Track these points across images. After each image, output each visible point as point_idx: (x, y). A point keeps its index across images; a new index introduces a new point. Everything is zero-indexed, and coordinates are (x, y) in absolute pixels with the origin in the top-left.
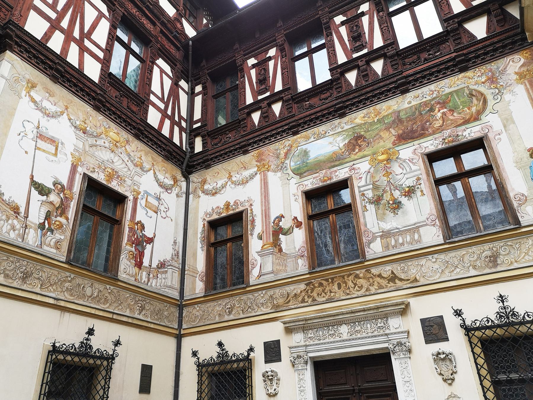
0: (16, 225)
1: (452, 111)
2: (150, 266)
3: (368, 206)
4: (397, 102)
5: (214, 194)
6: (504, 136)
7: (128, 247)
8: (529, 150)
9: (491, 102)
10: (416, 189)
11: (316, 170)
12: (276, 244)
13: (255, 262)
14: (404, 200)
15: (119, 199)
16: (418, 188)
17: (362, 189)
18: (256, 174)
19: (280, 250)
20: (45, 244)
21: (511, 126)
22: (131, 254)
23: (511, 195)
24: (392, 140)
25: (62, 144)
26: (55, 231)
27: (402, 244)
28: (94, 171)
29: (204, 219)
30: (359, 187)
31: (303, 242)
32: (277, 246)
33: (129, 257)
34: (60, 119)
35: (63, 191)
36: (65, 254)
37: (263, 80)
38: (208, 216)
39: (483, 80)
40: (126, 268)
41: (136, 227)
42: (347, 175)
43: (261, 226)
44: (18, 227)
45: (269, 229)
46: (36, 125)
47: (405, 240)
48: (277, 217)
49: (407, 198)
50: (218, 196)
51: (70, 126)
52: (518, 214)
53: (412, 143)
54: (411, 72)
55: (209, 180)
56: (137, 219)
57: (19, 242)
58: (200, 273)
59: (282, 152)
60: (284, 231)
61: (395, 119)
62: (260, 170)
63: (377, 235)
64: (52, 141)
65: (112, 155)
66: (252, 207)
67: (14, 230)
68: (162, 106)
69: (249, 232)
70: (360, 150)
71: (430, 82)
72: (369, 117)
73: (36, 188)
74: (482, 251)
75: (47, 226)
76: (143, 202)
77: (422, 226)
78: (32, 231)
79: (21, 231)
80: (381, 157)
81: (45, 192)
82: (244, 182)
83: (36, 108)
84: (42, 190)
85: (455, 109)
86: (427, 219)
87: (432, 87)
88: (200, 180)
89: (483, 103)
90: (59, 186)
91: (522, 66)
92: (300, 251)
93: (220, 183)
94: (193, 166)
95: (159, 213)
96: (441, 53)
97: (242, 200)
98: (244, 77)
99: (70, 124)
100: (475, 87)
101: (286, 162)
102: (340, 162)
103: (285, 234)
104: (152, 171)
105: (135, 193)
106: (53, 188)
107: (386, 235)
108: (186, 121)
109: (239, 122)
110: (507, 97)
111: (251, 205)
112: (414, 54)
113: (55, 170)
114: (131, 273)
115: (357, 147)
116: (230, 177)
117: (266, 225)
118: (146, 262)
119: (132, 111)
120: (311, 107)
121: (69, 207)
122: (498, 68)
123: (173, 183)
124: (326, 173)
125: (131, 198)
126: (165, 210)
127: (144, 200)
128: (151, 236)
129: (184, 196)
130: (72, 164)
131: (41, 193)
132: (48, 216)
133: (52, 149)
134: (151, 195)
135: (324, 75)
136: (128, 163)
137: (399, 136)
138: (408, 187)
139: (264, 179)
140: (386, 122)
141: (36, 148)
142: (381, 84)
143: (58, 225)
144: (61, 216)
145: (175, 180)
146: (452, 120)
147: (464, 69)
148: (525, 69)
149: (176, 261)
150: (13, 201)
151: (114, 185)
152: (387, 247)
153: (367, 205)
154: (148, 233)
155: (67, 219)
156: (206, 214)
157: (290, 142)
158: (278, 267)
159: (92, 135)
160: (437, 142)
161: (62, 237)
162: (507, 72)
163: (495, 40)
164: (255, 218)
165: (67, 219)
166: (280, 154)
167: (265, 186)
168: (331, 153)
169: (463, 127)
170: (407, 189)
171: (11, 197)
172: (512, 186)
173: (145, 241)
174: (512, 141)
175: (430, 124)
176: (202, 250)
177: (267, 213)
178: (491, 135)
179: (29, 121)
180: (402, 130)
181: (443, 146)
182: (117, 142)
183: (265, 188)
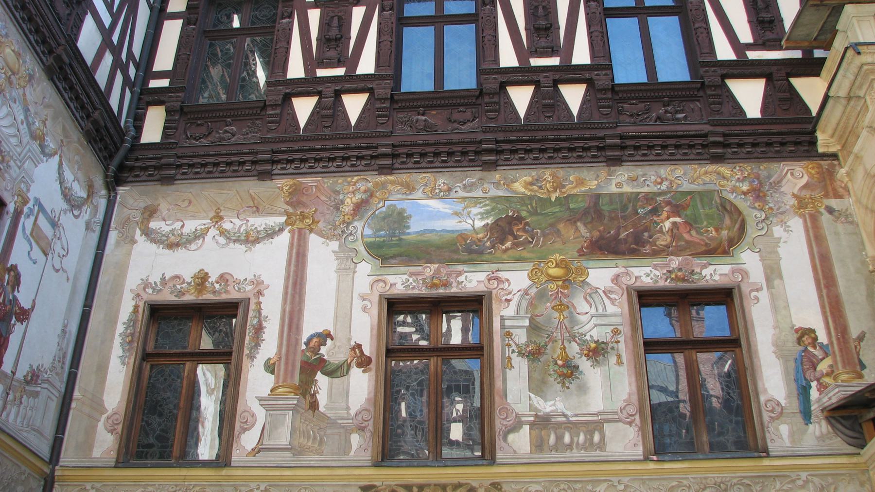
1: (690, 224)
2: (14, 373)
3: (516, 360)
4: (598, 176)
5: (172, 246)
6: (764, 295)
8: (797, 331)
9: (751, 232)
10: (609, 350)
11: (419, 259)
12: (305, 389)
13: (250, 419)
14: (585, 364)
16: (613, 348)
17: (508, 323)
18: (281, 230)
19: (314, 406)
21: (776, 282)
23: (763, 399)
24: (580, 247)
27: (570, 447)
29: (138, 295)
30: (502, 318)
31: (368, 400)
32: (308, 397)
37: (334, 43)
38: (150, 291)
39: (745, 188)
41: (7, 277)
42: (482, 288)
43: (275, 343)
45: (295, 354)
47: (575, 439)
48: (318, 335)
49: (589, 363)
50: (180, 252)
52: (767, 435)
53: (615, 262)
54: (632, 130)
55: (165, 213)
56: (12, 261)
58: (110, 412)
59: (348, 200)
60: (330, 368)
61: (589, 207)
62: (293, 224)
63: (523, 419)
66: (261, 299)
68: (107, 20)
69: (246, 351)
70: (516, 245)
71: (659, 160)
72: (540, 187)
74: (702, 486)
77: (609, 421)
80: (554, 272)
82: (250, 239)
85: (696, 222)
86: (621, 410)
87: (664, 170)
88: (142, 205)
89: (739, 229)
91: (806, 186)
92: (359, 418)
93: (191, 226)
94: (132, 169)
95: (50, 256)
96: (685, 117)
97: (239, 275)
98: (291, 16)
100: (731, 197)
101: (356, 224)
102: (470, 257)
103: (330, 373)
104: (57, 157)
107: (542, 422)
108: (137, 67)
109: (264, 107)
110: (778, 231)
111: (260, 293)
112: (641, 100)
115: (510, 237)
116: (218, 218)
117: (288, 346)
119: (57, 14)
120: (428, 127)
122: (769, 177)
123: (85, 196)
124: (438, 271)
125: (11, 207)
126: (63, 253)
127: (32, 218)
128: (26, 304)
129: (98, 229)
135: (461, 76)
136: (21, 127)
137: (591, 241)
138: (596, 342)
139: (299, 245)
140: (572, 206)
142: (575, 134)
145: (91, 191)
146: (687, 242)
147: (717, 159)
148: (807, 194)
149: (57, 374)
152: (538, 445)
153: (514, 356)
156: (146, 285)
157: (370, 185)
158: (303, 441)
160: (658, 273)
162: (783, 189)
163: (775, 129)
164: (265, 324)
166: (342, 202)
167: (297, 261)
168: (455, 235)
169: (704, 261)
170: (593, 345)
172: (764, 385)
173: (16, 314)
174: (775, 309)
175: (651, 237)
176: (123, 363)
177: (295, 320)
178: (745, 289)
180: (599, 231)
181: (667, 284)
182: (13, 73)
183: (297, 266)
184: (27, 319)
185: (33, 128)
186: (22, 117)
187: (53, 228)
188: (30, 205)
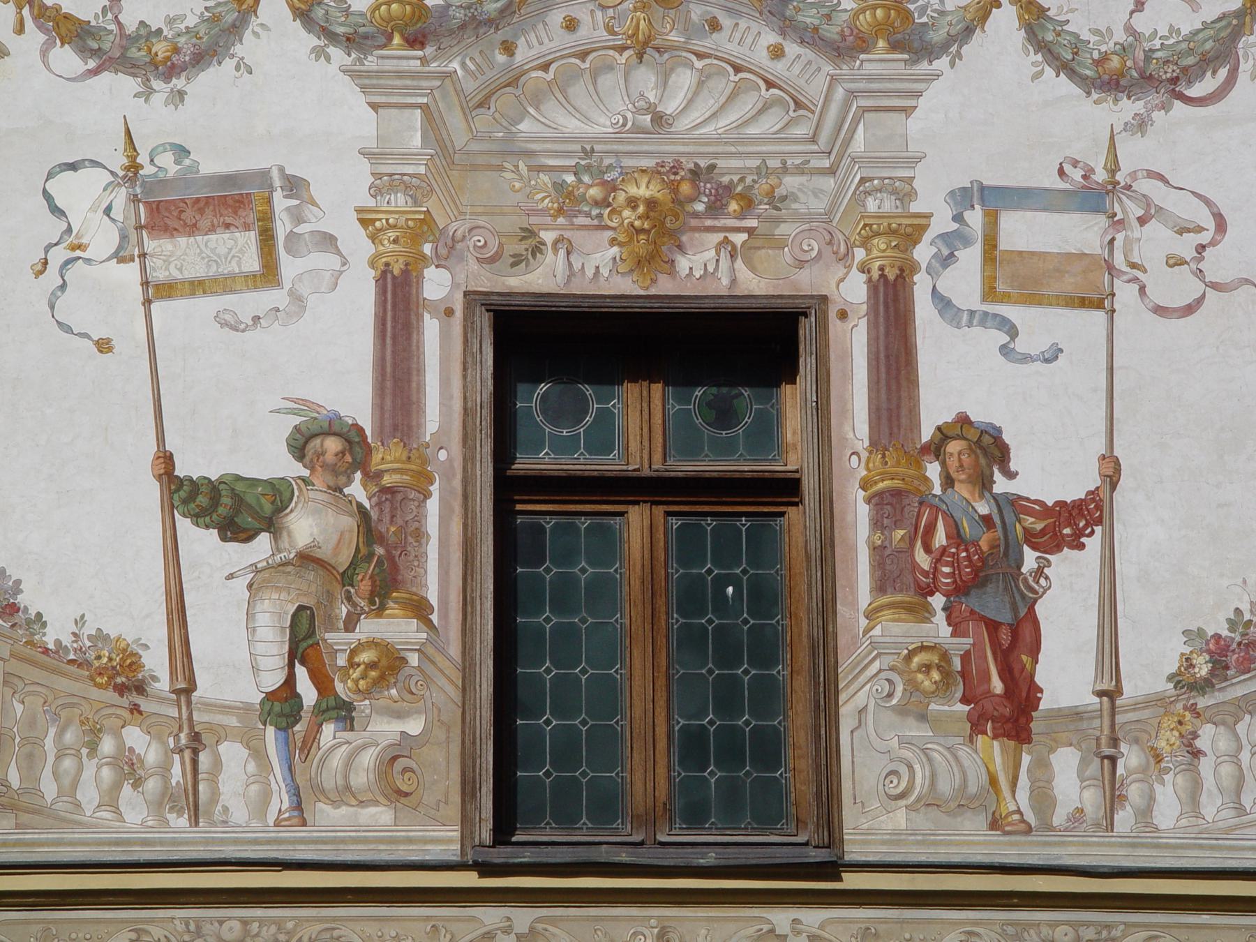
0: (140, 750)
2: (1111, 695)
7: (896, 631)
15: (756, 346)
20: (320, 792)
22: (927, 668)
25: (294, 185)
26: (363, 705)
28: (537, 249)
33: (913, 687)
34: (247, 47)
35: (362, 463)
36: (453, 809)
40: (896, 771)
41: (933, 470)
44: (152, 756)
46: (118, 161)
51: (319, 53)
56: (933, 413)
57: (179, 833)
64: (235, 202)
65: (646, 80)
67: (137, 783)
73: (200, 517)
75: (307, 691)
76: (964, 279)
78: (233, 754)
79: (176, 770)
81: (256, 515)
83: (92, 64)
84: (234, 509)
90: (332, 445)
95: (1125, 294)
99: (314, 41)
105: (880, 243)
106: (295, 469)
113: (292, 358)
114: (946, 786)
118: (1064, 676)
121: (420, 535)
126: (1185, 246)
127: (970, 258)
128: (1069, 484)
130: (381, 280)
131: (234, 530)
132: (303, 644)
133: (236, 248)
134: (1022, 197)
141: (156, 291)
143: (372, 666)
144: (380, 612)
150: (100, 637)
151: (707, 269)
154: (1045, 472)
155: (420, 609)
159: (476, 24)
161: (414, 727)
165: (420, 609)
171: (80, 621)
173: (1031, 538)
179: (73, 167)
184: (1099, 522)
185: (831, 32)
186: (770, 38)
187: (1097, 210)
188: (942, 222)
